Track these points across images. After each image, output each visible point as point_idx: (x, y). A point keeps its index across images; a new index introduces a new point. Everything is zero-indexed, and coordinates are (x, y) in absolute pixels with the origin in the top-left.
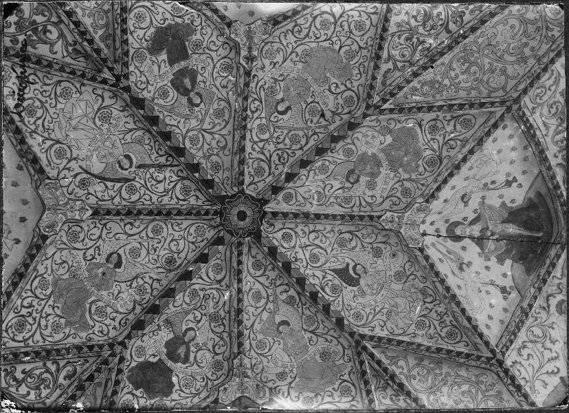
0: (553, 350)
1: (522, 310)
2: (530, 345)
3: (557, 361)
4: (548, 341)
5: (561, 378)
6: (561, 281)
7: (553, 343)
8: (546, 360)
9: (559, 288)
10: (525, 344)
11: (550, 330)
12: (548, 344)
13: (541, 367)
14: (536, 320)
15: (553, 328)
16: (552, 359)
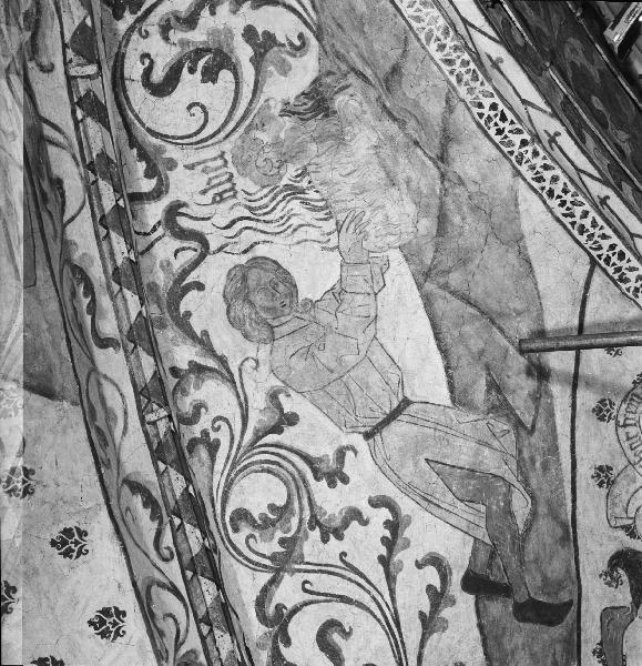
0: (367, 511)
1: (149, 501)
2: (288, 592)
3: (407, 533)
4: (320, 489)
5: (472, 583)
6: (165, 202)
7: (336, 477)
8: (377, 574)
9: (182, 234)
10: (271, 610)
11: (289, 436)
12: (331, 501)
13: (393, 627)
14: (213, 448)
15: (292, 420)
16: (390, 544)
